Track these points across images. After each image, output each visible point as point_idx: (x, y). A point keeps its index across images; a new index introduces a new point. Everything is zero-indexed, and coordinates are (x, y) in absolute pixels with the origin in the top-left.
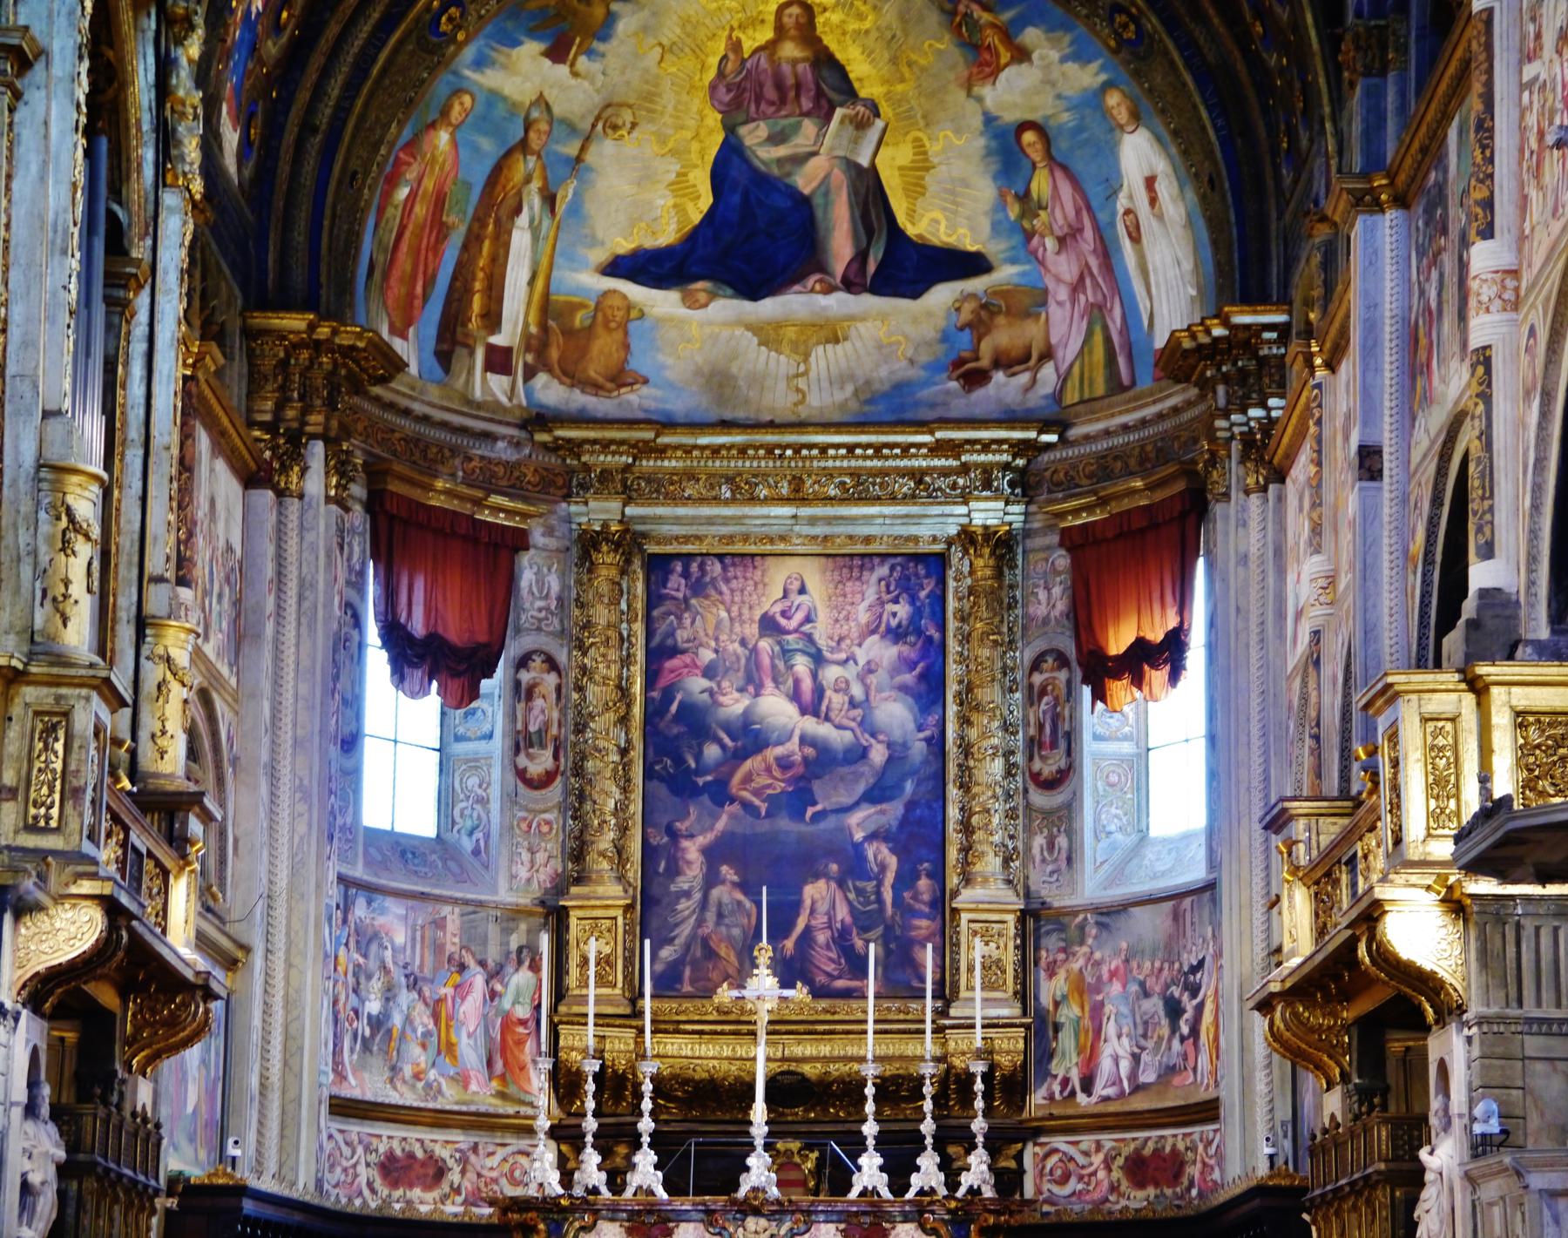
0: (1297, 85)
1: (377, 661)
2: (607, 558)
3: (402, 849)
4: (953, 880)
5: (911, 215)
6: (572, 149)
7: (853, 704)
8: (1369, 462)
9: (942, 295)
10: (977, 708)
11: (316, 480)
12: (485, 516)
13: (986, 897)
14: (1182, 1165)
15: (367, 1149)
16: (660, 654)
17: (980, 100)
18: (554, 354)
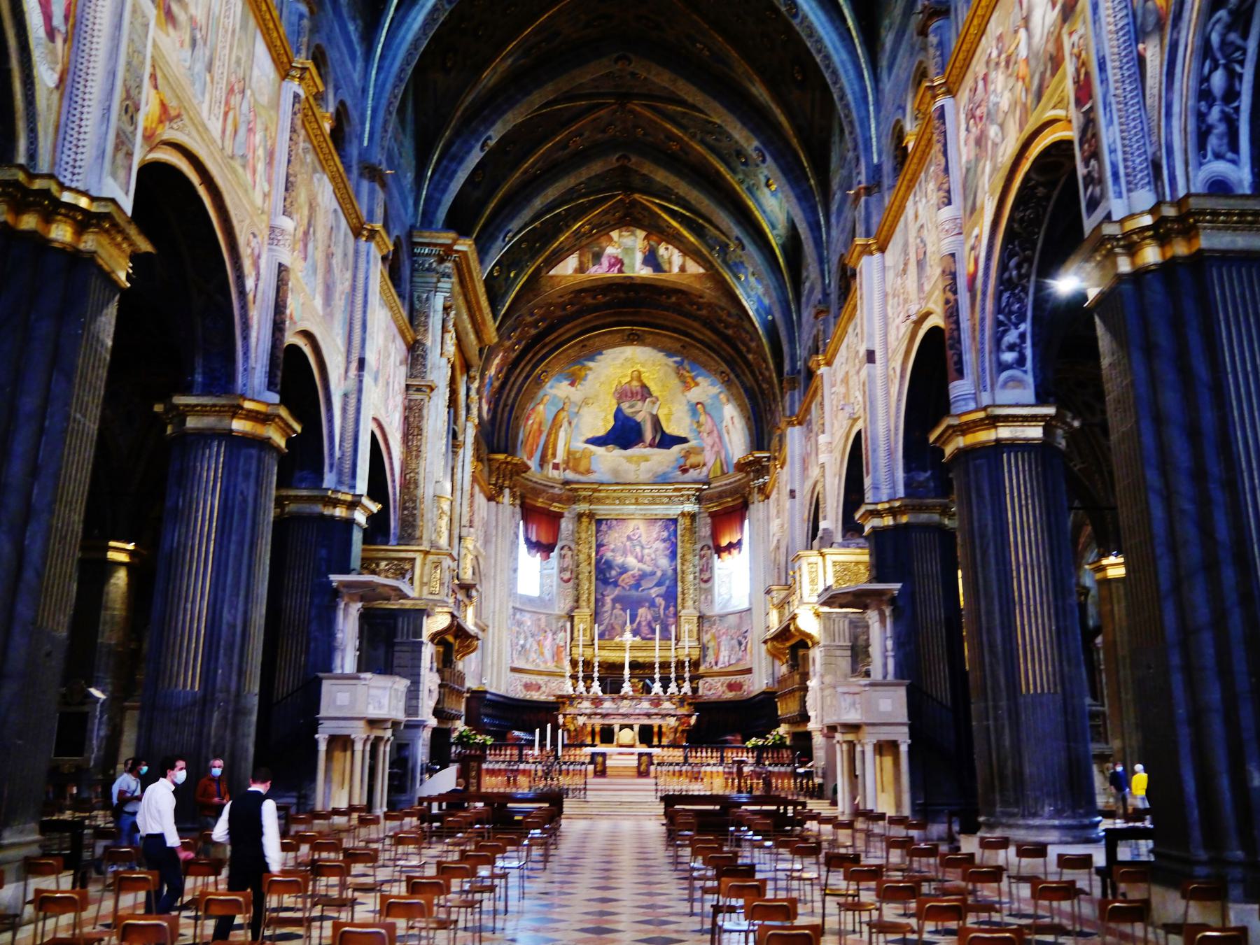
2: (585, 520)
3: (530, 600)
4: (679, 608)
8: (792, 494)
11: (506, 498)
13: (688, 614)
16: (599, 546)
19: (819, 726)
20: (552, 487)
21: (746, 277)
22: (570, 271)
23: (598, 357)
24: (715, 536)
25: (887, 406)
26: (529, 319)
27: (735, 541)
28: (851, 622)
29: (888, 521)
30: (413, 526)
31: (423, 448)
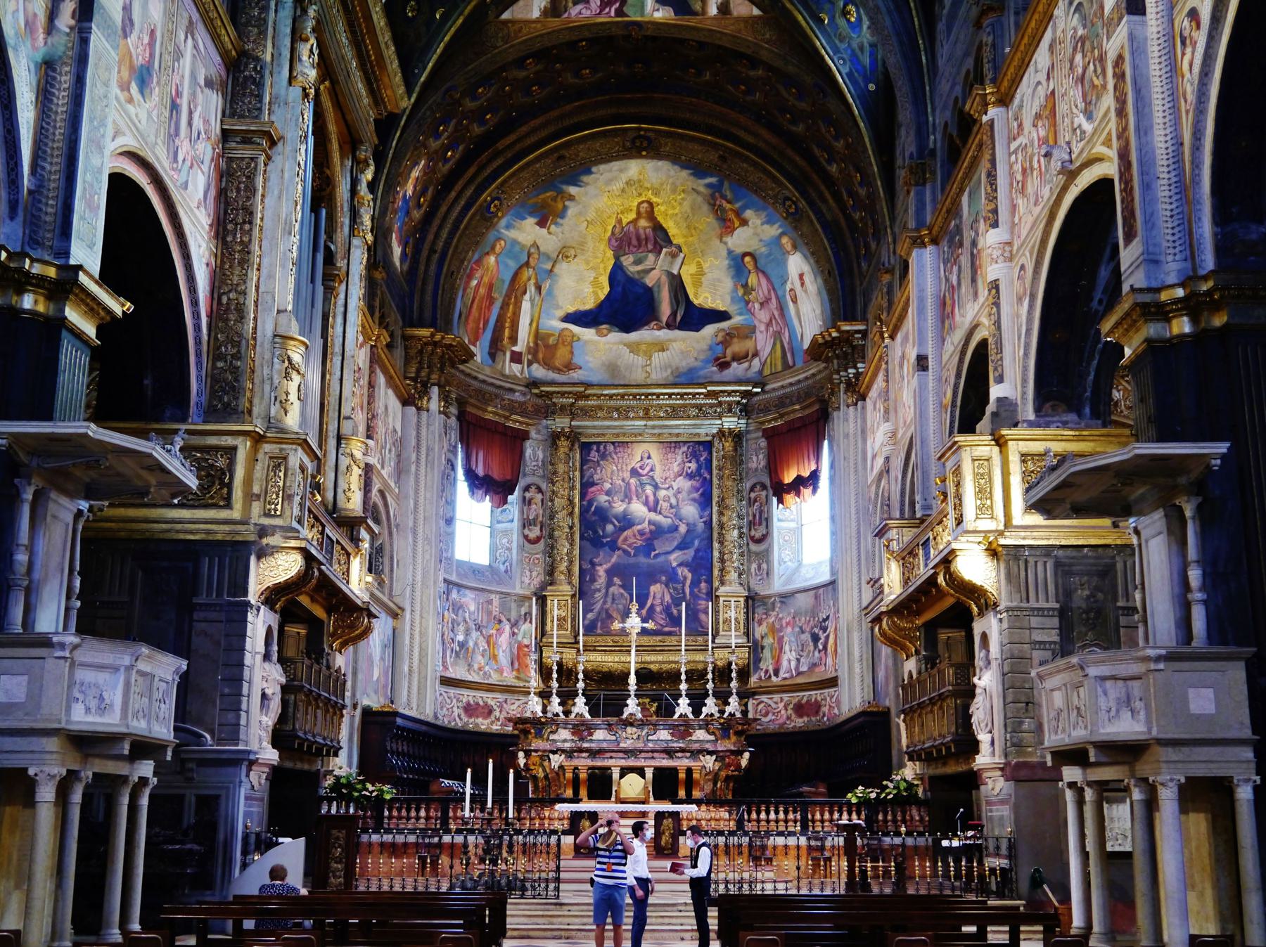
0: (870, 223)
1: (462, 486)
2: (563, 443)
3: (475, 570)
4: (716, 583)
5: (696, 295)
6: (548, 266)
7: (672, 507)
8: (922, 363)
9: (709, 330)
10: (727, 508)
11: (434, 402)
12: (510, 424)
13: (731, 592)
14: (820, 706)
15: (458, 701)
16: (587, 485)
17: (726, 243)
18: (541, 356)
19: (999, 759)
20: (511, 390)
21: (832, 19)
22: (536, 14)
23: (585, 178)
24: (774, 466)
25: (1174, 96)
26: (469, 104)
27: (806, 474)
28: (1058, 565)
29: (1182, 326)
31: (255, 247)
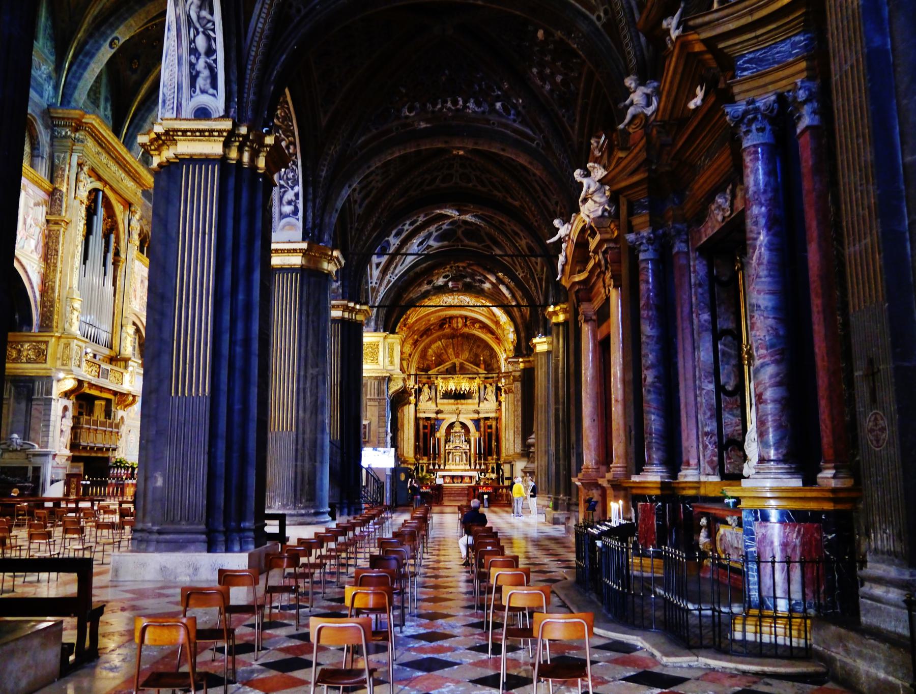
30: (51, 320)
